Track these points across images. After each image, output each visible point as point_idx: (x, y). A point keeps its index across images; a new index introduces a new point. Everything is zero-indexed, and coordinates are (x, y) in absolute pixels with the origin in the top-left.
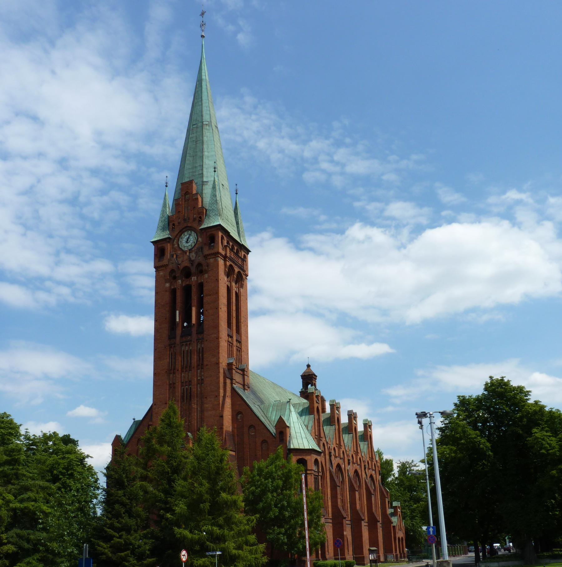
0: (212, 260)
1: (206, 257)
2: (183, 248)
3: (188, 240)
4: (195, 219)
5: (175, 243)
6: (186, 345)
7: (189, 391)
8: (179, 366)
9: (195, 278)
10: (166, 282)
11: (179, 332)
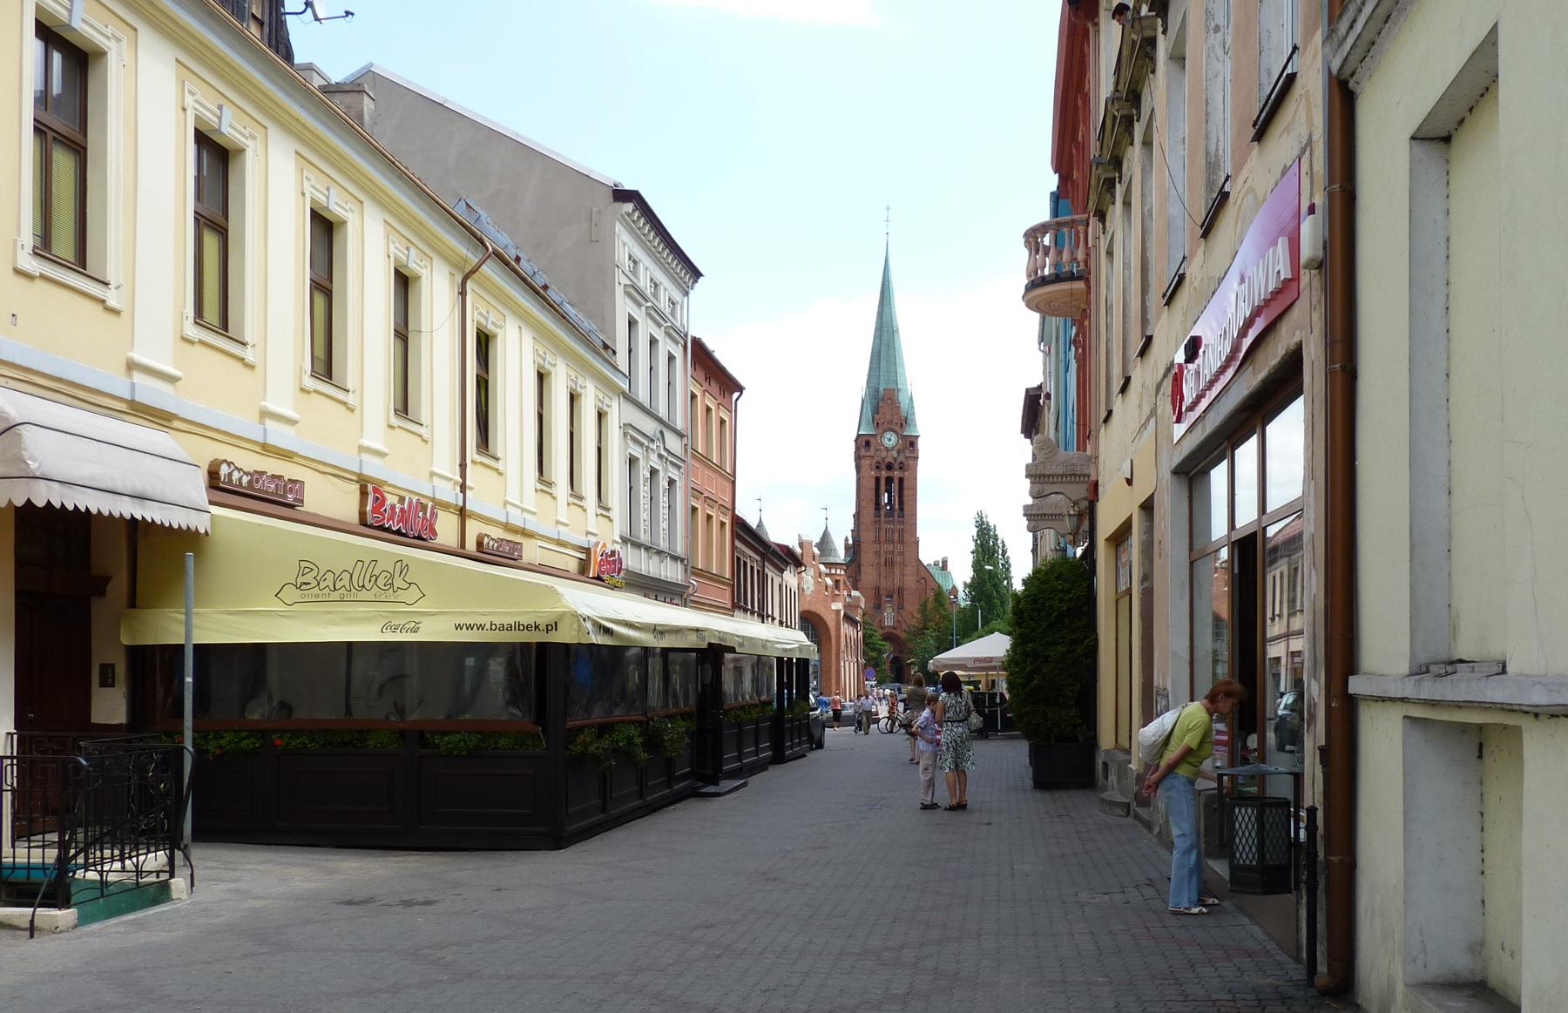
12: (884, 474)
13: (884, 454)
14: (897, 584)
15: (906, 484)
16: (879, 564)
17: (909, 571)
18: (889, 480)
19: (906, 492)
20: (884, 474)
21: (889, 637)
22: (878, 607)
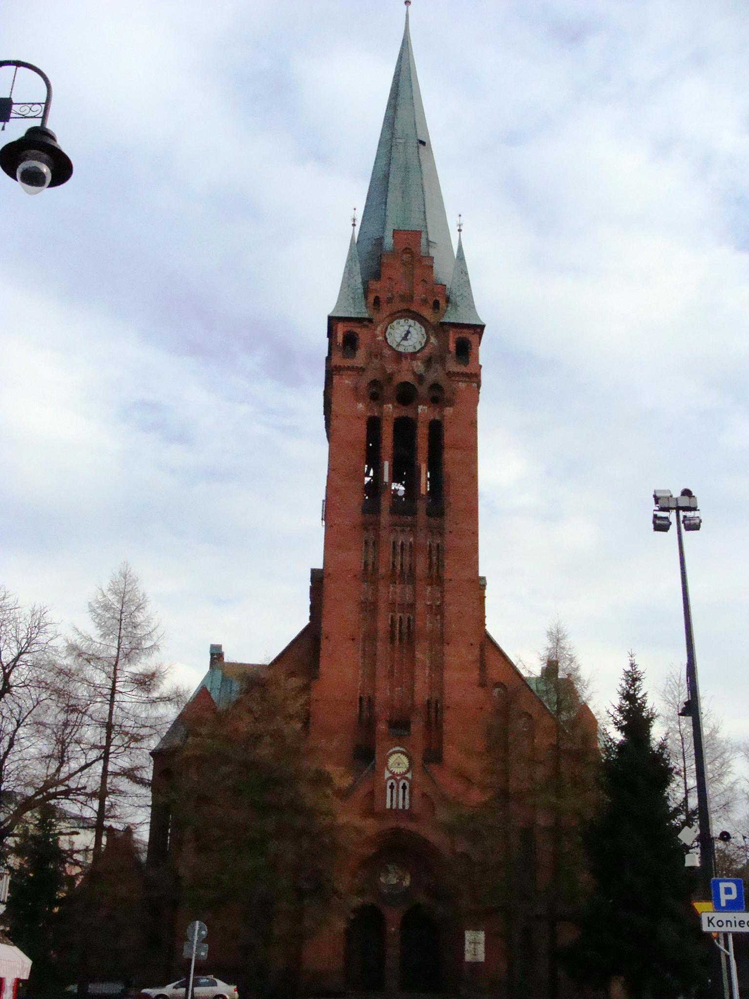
0: (462, 385)
1: (450, 374)
3: (407, 335)
4: (424, 301)
6: (403, 531)
7: (405, 624)
8: (382, 570)
11: (385, 503)
13: (390, 368)
15: (449, 436)
16: (371, 636)
18: (405, 429)
19: (449, 455)
21: (398, 845)
22: (365, 756)
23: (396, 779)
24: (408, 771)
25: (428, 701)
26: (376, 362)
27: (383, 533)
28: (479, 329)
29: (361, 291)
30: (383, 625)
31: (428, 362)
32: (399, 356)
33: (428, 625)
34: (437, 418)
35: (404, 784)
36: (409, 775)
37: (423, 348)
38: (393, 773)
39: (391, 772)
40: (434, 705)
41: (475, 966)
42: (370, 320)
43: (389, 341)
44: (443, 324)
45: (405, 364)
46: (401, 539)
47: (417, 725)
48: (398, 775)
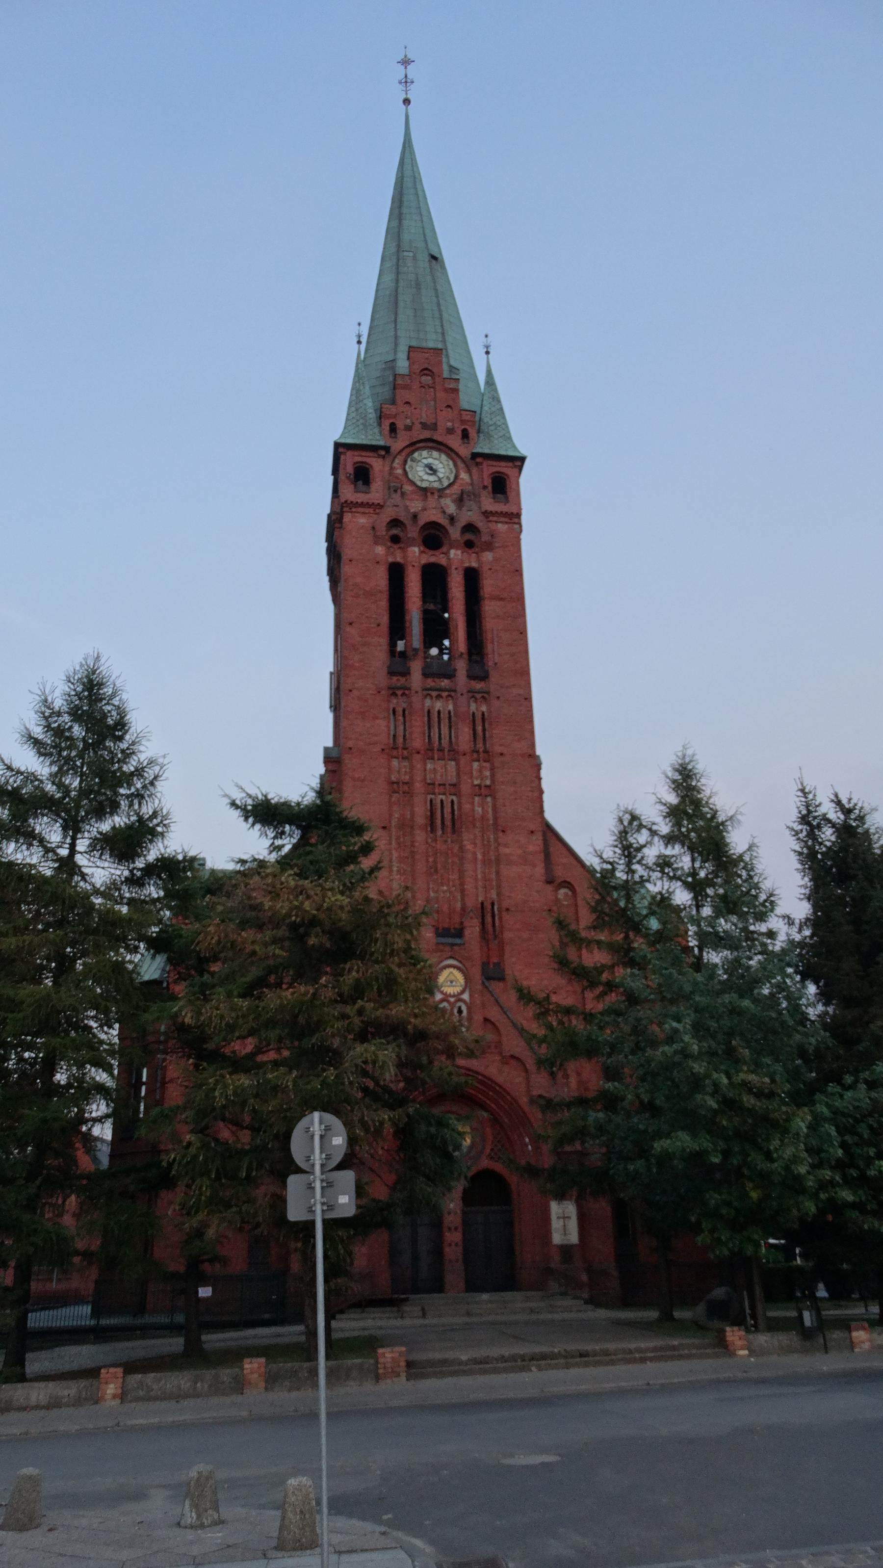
1: (487, 514)
2: (419, 483)
3: (431, 469)
4: (450, 431)
5: (395, 465)
6: (439, 697)
7: (447, 810)
8: (417, 742)
9: (459, 552)
10: (376, 543)
12: (416, 556)
13: (415, 505)
14: (476, 895)
15: (488, 585)
17: (519, 845)
19: (490, 608)
20: (416, 556)
23: (448, 1002)
24: (463, 992)
25: (482, 903)
26: (397, 497)
27: (414, 699)
28: (518, 461)
29: (372, 415)
30: (420, 812)
31: (460, 500)
32: (425, 492)
33: (479, 810)
34: (474, 564)
35: (460, 1008)
36: (466, 996)
37: (450, 485)
38: (445, 994)
39: (442, 992)
40: (489, 907)
41: (566, 1250)
42: (387, 449)
43: (410, 476)
44: (475, 456)
45: (432, 501)
46: (438, 705)
47: (472, 931)
48: (450, 996)
